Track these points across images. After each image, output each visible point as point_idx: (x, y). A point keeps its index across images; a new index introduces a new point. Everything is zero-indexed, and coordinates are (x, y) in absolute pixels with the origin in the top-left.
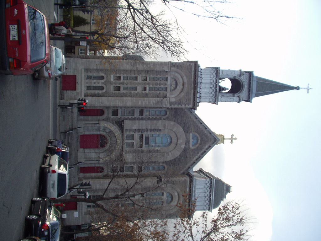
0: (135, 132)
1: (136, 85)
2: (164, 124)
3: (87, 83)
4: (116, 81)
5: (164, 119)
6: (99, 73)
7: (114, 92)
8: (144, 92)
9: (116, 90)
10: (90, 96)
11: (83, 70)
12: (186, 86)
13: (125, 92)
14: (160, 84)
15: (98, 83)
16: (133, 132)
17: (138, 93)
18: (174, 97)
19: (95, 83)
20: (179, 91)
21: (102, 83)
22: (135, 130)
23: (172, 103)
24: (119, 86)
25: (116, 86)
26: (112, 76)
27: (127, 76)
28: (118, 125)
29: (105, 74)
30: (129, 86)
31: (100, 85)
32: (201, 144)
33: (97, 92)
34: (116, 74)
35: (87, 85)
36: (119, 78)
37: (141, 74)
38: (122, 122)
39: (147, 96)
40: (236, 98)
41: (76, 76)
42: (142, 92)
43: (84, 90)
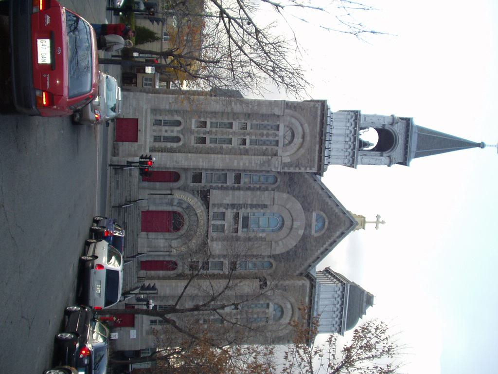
0: (227, 209)
1: (231, 136)
2: (272, 196)
3: (154, 131)
4: (200, 129)
6: (173, 116)
7: (196, 145)
8: (242, 147)
9: (199, 143)
10: (159, 151)
11: (149, 111)
12: (308, 138)
13: (212, 145)
14: (268, 135)
15: (172, 131)
17: (233, 148)
18: (289, 156)
19: (166, 131)
20: (297, 146)
21: (178, 131)
22: (228, 204)
23: (285, 165)
24: (204, 136)
25: (199, 137)
26: (193, 121)
29: (183, 118)
30: (219, 136)
31: (175, 134)
32: (328, 229)
33: (169, 145)
34: (200, 117)
35: (155, 134)
36: (204, 124)
38: (207, 192)
39: (246, 152)
40: (385, 159)
41: (137, 119)
43: (150, 142)
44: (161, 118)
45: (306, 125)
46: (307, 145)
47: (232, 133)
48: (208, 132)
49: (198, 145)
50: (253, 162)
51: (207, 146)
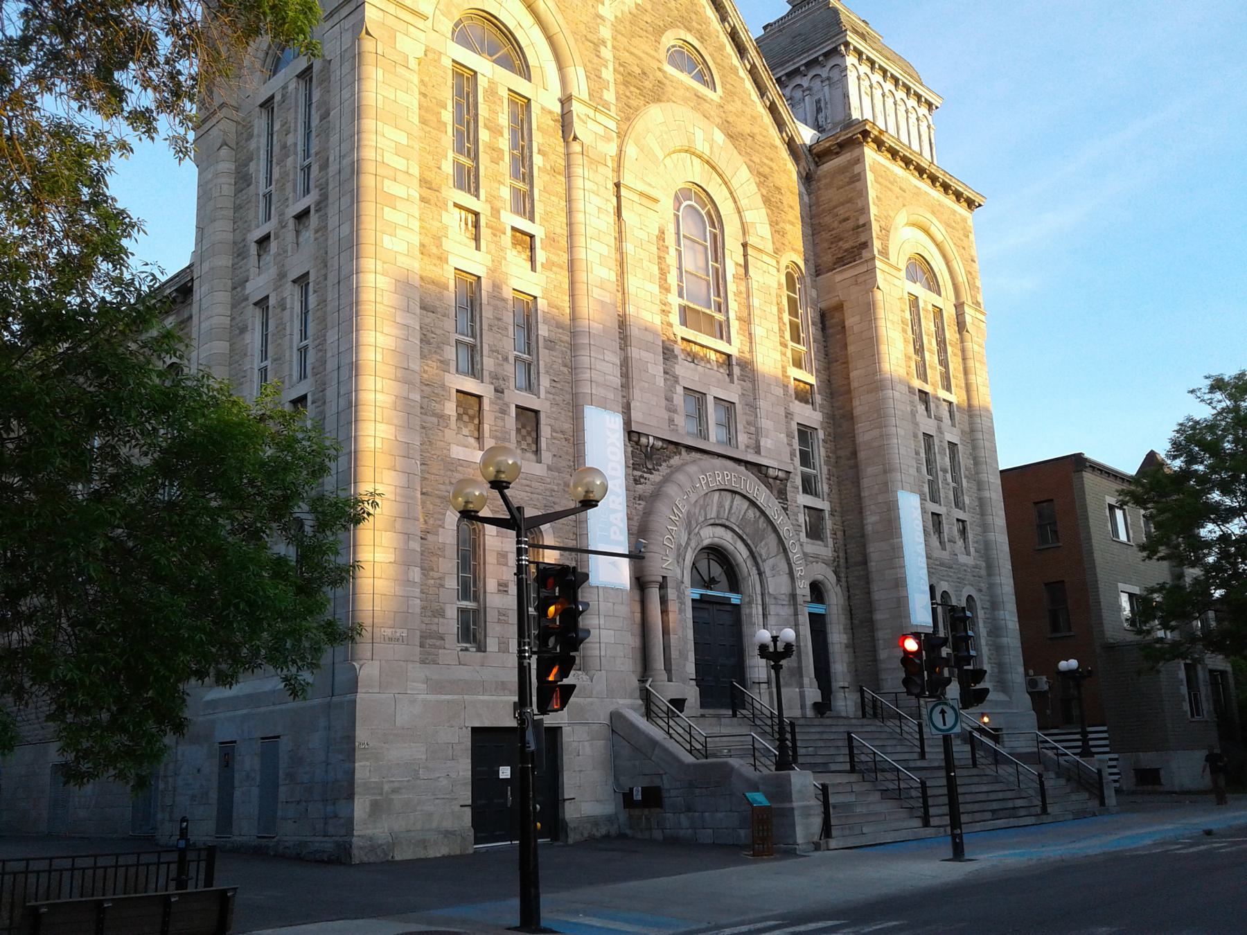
2: (636, 198)
4: (486, 427)
13: (545, 382)
14: (496, 131)
20: (528, 20)
22: (665, 373)
25: (518, 431)
27: (454, 344)
32: (702, 39)
38: (637, 443)
41: (475, 730)
44: (452, 613)
48: (496, 390)
51: (548, 403)
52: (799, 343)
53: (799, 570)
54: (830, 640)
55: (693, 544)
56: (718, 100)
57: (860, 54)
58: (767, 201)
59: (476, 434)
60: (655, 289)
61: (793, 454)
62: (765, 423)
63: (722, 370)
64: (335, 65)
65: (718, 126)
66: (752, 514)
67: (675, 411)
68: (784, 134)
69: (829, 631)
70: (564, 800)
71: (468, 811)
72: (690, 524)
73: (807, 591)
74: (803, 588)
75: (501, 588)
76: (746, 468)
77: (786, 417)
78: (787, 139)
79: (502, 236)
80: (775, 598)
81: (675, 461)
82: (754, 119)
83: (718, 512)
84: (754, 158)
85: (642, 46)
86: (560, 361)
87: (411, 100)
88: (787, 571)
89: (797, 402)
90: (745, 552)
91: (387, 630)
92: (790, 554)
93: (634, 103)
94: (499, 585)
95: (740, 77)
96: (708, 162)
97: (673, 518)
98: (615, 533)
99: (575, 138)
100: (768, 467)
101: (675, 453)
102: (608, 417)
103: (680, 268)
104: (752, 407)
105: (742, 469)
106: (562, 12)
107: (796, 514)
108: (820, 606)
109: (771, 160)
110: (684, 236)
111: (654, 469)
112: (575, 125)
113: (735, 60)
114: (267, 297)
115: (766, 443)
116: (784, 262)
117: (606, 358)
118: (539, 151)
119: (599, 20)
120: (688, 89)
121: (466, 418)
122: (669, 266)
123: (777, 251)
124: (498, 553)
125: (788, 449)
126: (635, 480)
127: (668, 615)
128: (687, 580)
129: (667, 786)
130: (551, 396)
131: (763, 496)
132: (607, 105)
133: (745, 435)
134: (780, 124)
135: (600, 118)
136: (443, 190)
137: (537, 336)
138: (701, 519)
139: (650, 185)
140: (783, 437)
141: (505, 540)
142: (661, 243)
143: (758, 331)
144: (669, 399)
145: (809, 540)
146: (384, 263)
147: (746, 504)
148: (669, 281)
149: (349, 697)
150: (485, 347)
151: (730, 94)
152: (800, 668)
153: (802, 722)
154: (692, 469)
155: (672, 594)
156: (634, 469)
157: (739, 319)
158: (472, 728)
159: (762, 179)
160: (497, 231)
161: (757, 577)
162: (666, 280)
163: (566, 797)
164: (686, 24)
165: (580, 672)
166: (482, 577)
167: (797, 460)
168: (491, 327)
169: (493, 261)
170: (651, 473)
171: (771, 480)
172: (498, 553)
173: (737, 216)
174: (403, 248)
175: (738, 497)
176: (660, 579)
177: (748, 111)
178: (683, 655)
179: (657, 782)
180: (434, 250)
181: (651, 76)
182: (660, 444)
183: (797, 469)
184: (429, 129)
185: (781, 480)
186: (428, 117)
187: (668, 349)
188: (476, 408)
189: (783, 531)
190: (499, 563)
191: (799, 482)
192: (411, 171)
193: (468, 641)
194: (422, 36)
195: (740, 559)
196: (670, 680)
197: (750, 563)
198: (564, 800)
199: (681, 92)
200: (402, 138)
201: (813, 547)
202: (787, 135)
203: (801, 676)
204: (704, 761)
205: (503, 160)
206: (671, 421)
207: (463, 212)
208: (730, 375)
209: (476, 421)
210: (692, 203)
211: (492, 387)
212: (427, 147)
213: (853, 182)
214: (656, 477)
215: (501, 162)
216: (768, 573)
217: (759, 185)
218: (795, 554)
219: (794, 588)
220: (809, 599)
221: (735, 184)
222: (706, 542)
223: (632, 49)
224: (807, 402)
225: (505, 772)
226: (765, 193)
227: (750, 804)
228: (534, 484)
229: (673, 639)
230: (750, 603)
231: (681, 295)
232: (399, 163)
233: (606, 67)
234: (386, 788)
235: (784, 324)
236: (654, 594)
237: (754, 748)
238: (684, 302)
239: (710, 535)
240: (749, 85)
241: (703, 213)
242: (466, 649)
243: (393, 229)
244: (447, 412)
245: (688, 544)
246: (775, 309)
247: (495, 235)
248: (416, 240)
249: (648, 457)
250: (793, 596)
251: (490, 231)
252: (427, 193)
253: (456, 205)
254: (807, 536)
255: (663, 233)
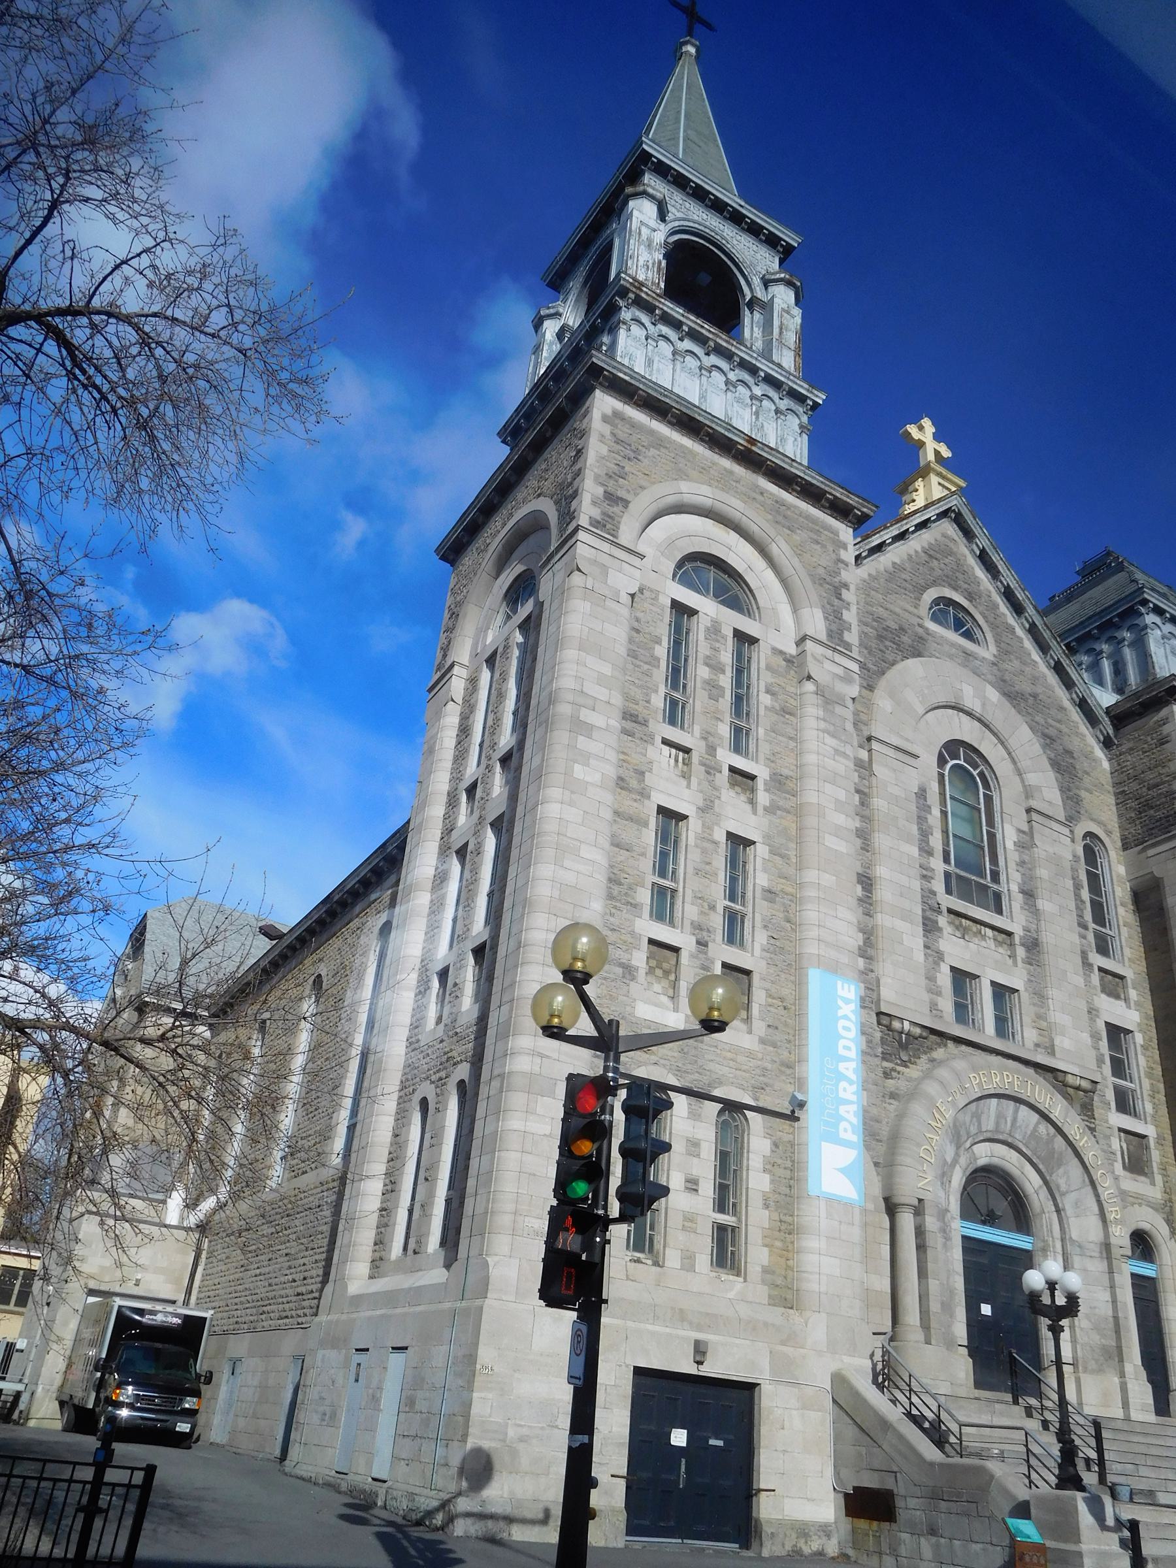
0: (940, 956)
2: (891, 752)
5: (861, 746)
7: (759, 1026)
8: (763, 798)
12: (735, 506)
14: (718, 668)
16: (937, 963)
17: (768, 838)
18: (795, 610)
20: (759, 563)
22: (926, 947)
23: (836, 639)
28: (904, 1064)
30: (717, 890)
32: (970, 597)
34: (629, 971)
35: (704, 1260)
37: (642, 773)
38: (889, 1028)
41: (638, 1371)
42: (760, 810)
45: (684, 486)
46: (757, 522)
47: (708, 828)
48: (698, 943)
49: (755, 1009)
50: (829, 763)
51: (764, 963)
52: (1104, 926)
53: (1113, 1213)
54: (1164, 1315)
55: (963, 1160)
56: (992, 658)
57: (1159, 611)
58: (1056, 765)
59: (671, 992)
60: (915, 851)
61: (1100, 1061)
62: (1058, 1017)
63: (1001, 950)
64: (546, 606)
65: (990, 683)
66: (1044, 1129)
67: (939, 994)
68: (1074, 696)
69: (1162, 1301)
70: (760, 1490)
71: (622, 1484)
72: (957, 1136)
73: (1127, 1242)
74: (1121, 1237)
75: (689, 1185)
76: (1036, 1071)
77: (1089, 1012)
78: (1077, 700)
79: (718, 775)
80: (1080, 1246)
81: (939, 1053)
82: (1035, 680)
83: (997, 1124)
84: (1037, 719)
85: (901, 604)
86: (781, 915)
87: (617, 634)
88: (1096, 1209)
89: (1103, 996)
90: (1036, 1180)
91: (534, 1220)
92: (1100, 1190)
93: (890, 656)
94: (687, 1181)
95: (1018, 637)
96: (979, 720)
97: (934, 1124)
98: (845, 1130)
99: (809, 678)
100: (1065, 1072)
101: (940, 1047)
102: (839, 984)
103: (945, 832)
104: (1040, 996)
105: (1031, 1071)
106: (798, 555)
107: (1108, 1137)
108: (1149, 1265)
109: (1059, 721)
110: (952, 798)
111: (910, 1061)
112: (809, 664)
113: (1010, 619)
114: (467, 844)
115: (1063, 1042)
116: (1080, 830)
117: (840, 915)
118: (767, 692)
119: (841, 565)
120: (953, 645)
121: (659, 972)
122: (930, 827)
123: (1070, 818)
124: (688, 1140)
125: (1093, 1053)
126: (885, 1073)
127: (925, 1252)
128: (955, 1206)
129: (900, 1489)
130: (768, 955)
131: (1058, 1108)
132: (848, 646)
133: (1035, 1031)
134: (1068, 684)
135: (838, 658)
136: (651, 723)
137: (754, 884)
138: (973, 1130)
139: (907, 740)
140: (1086, 1037)
141: (698, 1124)
142: (922, 802)
143: (1043, 904)
144: (931, 979)
145: (1128, 1174)
146: (572, 792)
147: (1035, 1117)
148: (931, 844)
149: (478, 1302)
150: (689, 892)
151: (1005, 652)
152: (1119, 1348)
153: (1119, 1425)
154: (960, 1065)
155: (931, 1223)
156: (884, 1059)
157: (1022, 892)
158: (635, 1367)
159: (1048, 741)
160: (711, 769)
161: (1055, 1216)
162: (928, 843)
163: (762, 1486)
164: (953, 583)
165: (791, 1311)
166: (666, 1168)
167: (1107, 1068)
168: (697, 872)
169: (705, 800)
170: (906, 1066)
171: (1070, 1091)
172: (688, 1140)
173: (1017, 778)
174: (596, 778)
175: (1023, 1108)
176: (916, 1202)
177: (1028, 670)
178: (947, 1307)
179: (889, 1484)
180: (634, 783)
181: (910, 631)
182: (917, 1031)
183: (1108, 1081)
184: (638, 663)
185: (1085, 1091)
186: (637, 651)
187: (929, 919)
188: (674, 962)
189: (1089, 1157)
190: (689, 1154)
191: (1110, 1096)
192: (612, 701)
193: (642, 1251)
194: (637, 573)
195: (1029, 1190)
196: (928, 1342)
197: (1044, 1193)
198: (760, 1490)
199: (946, 648)
200: (607, 669)
201: (1132, 1184)
202: (1078, 696)
203: (1121, 1360)
204: (957, 1460)
205: (723, 697)
206: (933, 1007)
207: (674, 751)
208: (1013, 956)
209: (672, 977)
210: (962, 762)
211: (693, 939)
212: (636, 681)
213: (1163, 744)
214: (913, 1072)
215: (720, 699)
216: (1069, 1210)
217: (1045, 747)
218: (1107, 1189)
219: (1107, 1235)
220: (1129, 1253)
221: (1012, 743)
222: (982, 1162)
223: (888, 606)
224: (1117, 997)
225: (679, 1438)
226: (1052, 755)
227: (1012, 1537)
228: (741, 1059)
229: (933, 1285)
230: (1044, 1250)
231: (946, 860)
232: (601, 693)
233: (848, 609)
234: (511, 1433)
235: (1083, 902)
236: (907, 1221)
237: (1028, 1450)
238: (952, 868)
239: (986, 1154)
240: (1028, 644)
241: (975, 773)
242: (638, 1261)
243: (585, 758)
244: (634, 963)
245: (955, 1161)
246: (1069, 884)
247: (708, 773)
248: (611, 772)
249: (903, 1046)
250: (1107, 1247)
251: (703, 768)
252: (629, 725)
253: (666, 742)
254: (1124, 1168)
255: (925, 791)
